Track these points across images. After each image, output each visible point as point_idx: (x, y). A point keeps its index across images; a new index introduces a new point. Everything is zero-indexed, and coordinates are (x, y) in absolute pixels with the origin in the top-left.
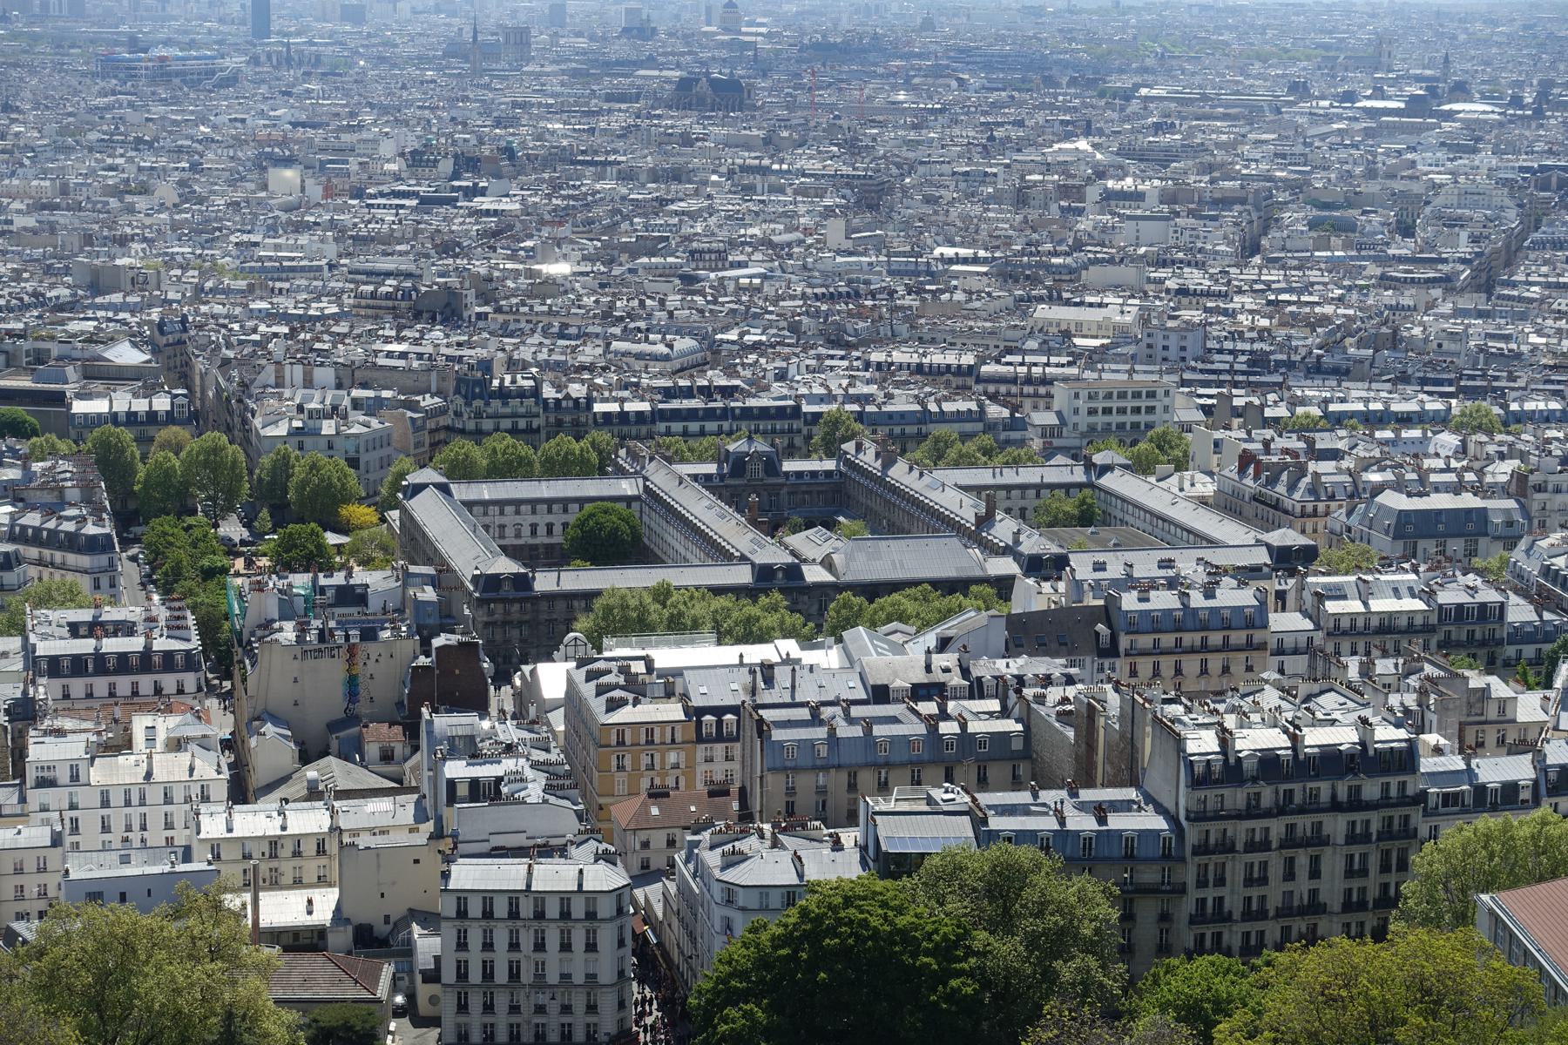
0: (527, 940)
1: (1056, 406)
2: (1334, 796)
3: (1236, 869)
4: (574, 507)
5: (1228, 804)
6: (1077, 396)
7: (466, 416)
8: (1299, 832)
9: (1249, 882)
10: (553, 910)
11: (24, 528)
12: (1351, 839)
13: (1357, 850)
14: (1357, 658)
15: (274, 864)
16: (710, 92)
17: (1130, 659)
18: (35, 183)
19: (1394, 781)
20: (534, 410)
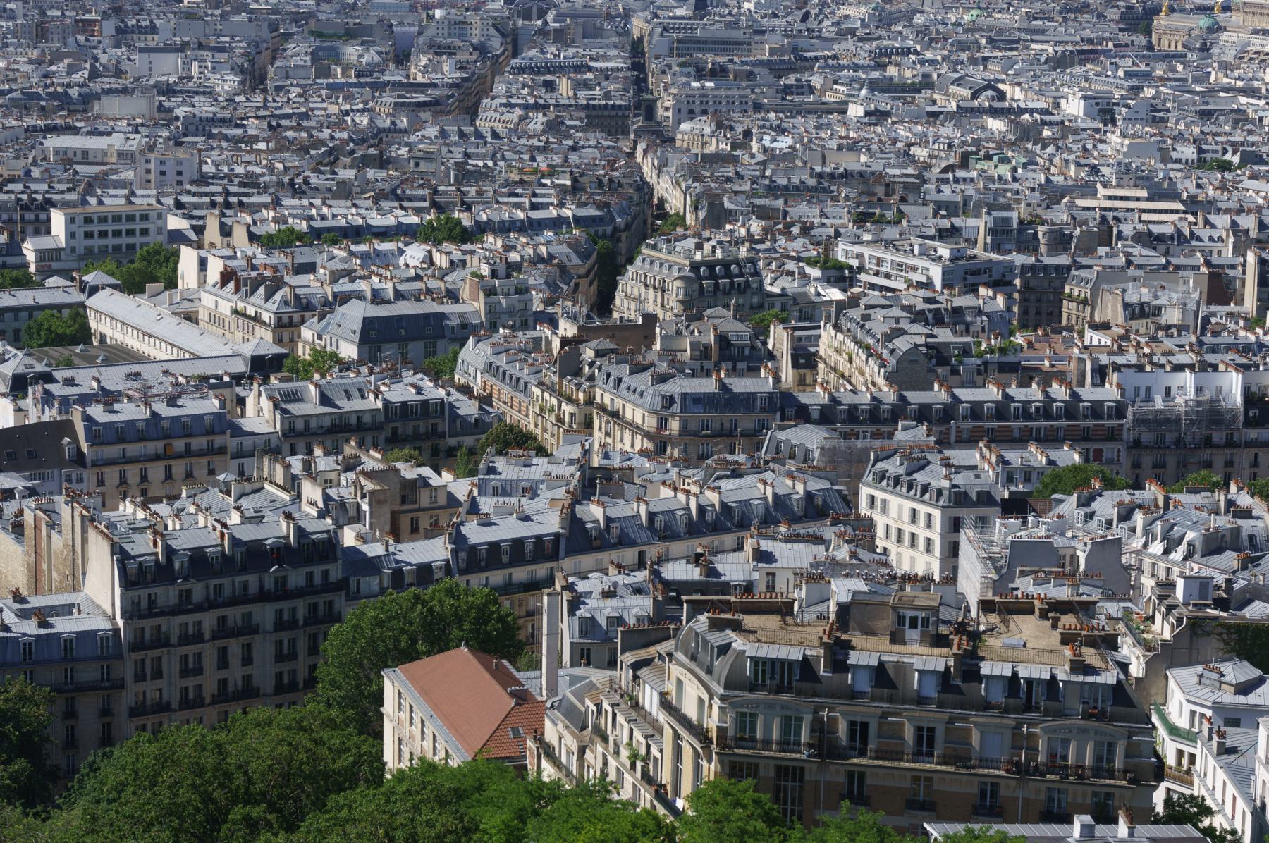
2: (262, 587)
3: (171, 661)
5: (161, 602)
8: (230, 622)
9: (185, 673)
12: (280, 625)
13: (285, 636)
14: (300, 457)
17: (96, 470)
19: (317, 570)
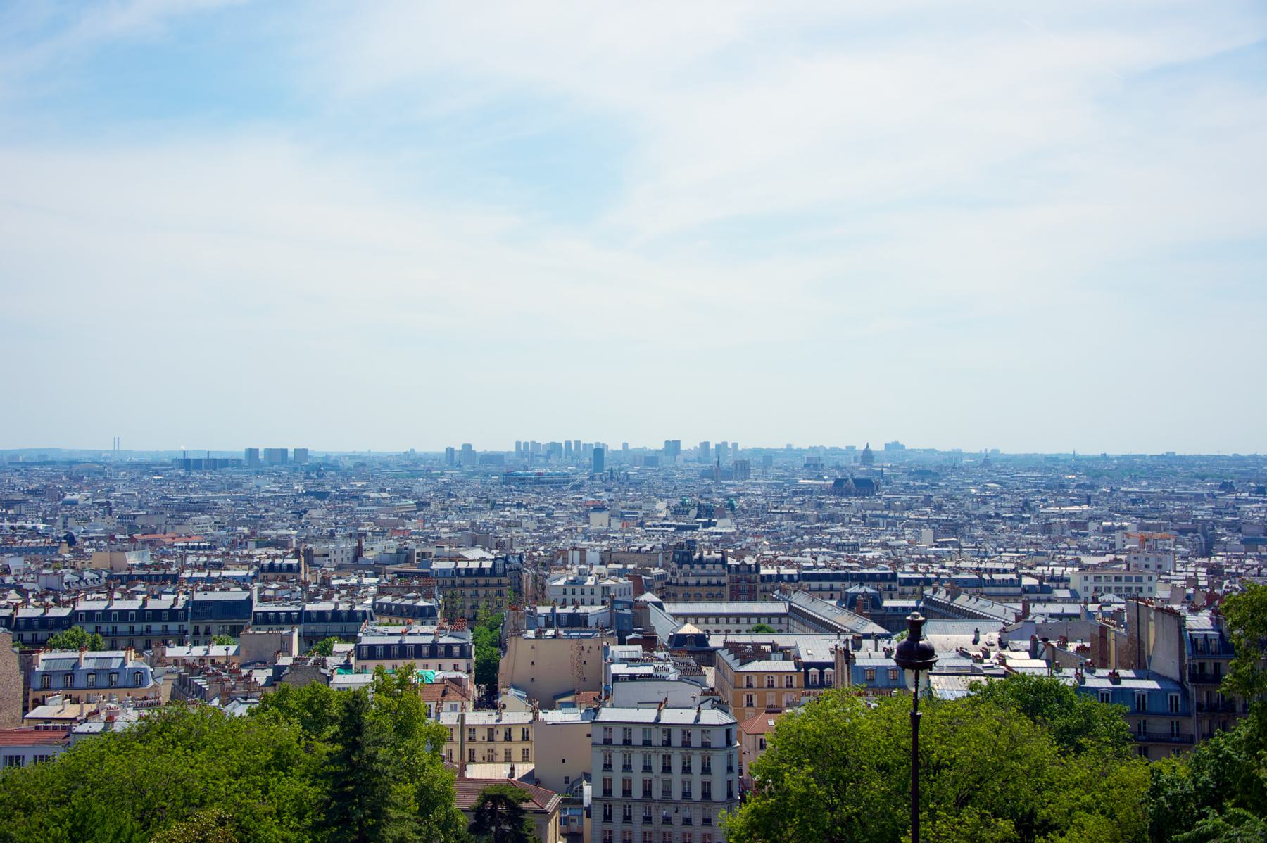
0: (657, 764)
1: (1071, 586)
4: (744, 620)
6: (1086, 578)
7: (678, 575)
10: (677, 740)
11: (381, 604)
15: (491, 746)
16: (854, 487)
18: (457, 522)
20: (723, 572)
